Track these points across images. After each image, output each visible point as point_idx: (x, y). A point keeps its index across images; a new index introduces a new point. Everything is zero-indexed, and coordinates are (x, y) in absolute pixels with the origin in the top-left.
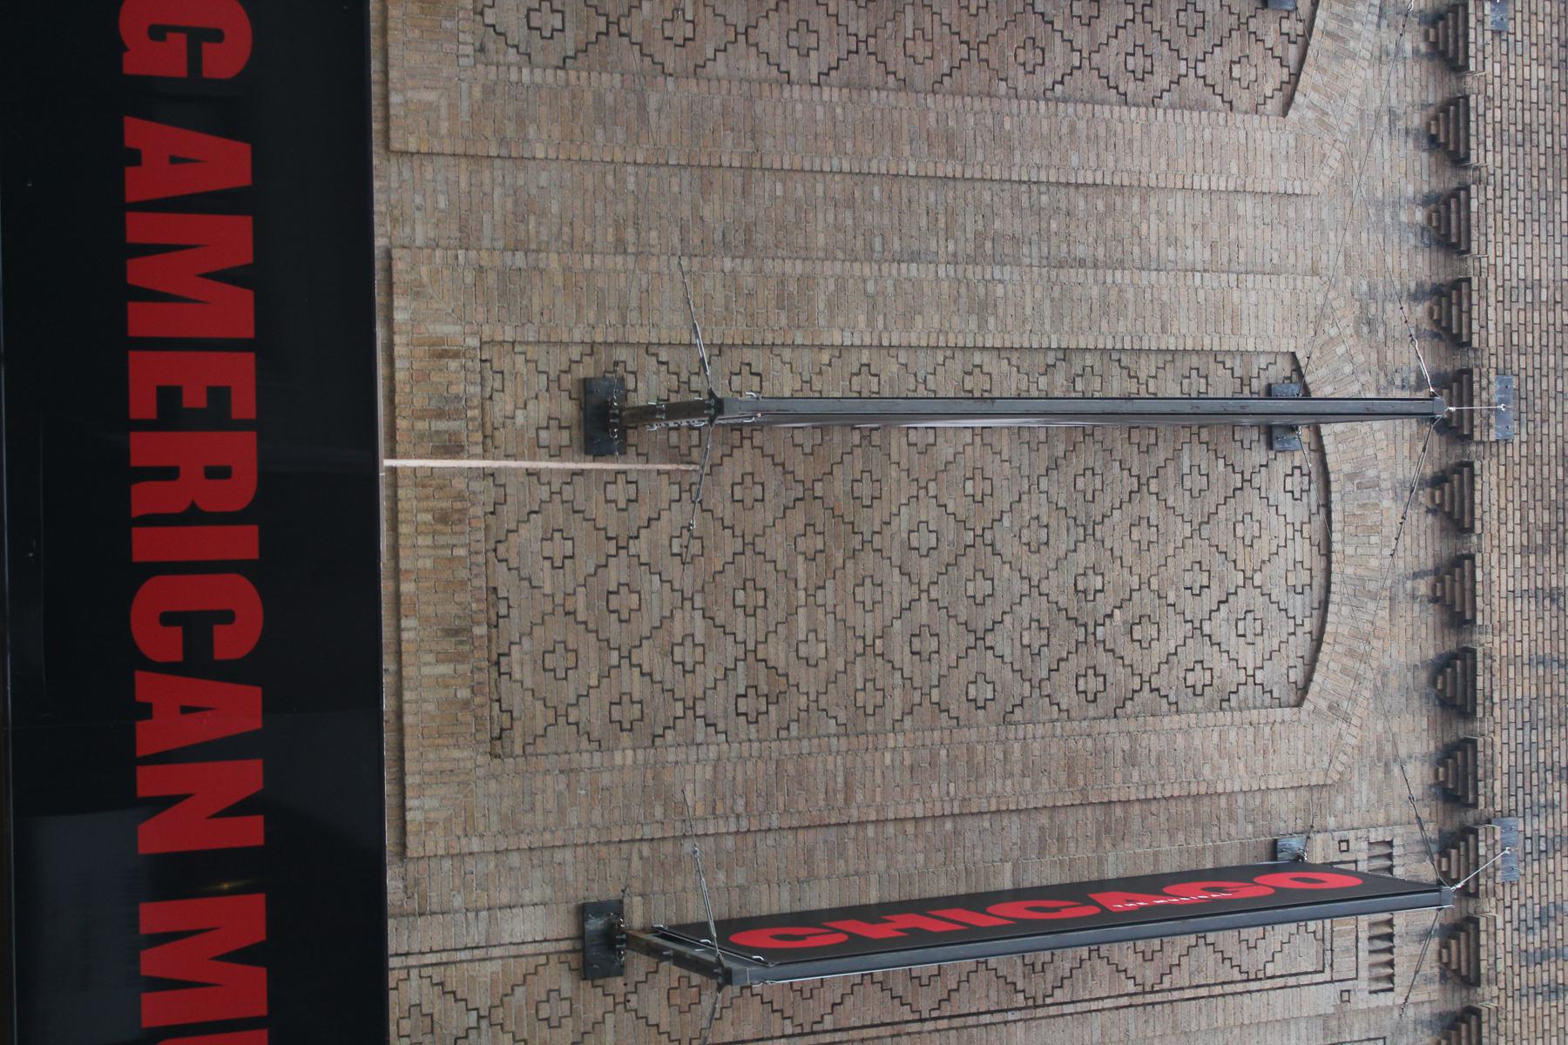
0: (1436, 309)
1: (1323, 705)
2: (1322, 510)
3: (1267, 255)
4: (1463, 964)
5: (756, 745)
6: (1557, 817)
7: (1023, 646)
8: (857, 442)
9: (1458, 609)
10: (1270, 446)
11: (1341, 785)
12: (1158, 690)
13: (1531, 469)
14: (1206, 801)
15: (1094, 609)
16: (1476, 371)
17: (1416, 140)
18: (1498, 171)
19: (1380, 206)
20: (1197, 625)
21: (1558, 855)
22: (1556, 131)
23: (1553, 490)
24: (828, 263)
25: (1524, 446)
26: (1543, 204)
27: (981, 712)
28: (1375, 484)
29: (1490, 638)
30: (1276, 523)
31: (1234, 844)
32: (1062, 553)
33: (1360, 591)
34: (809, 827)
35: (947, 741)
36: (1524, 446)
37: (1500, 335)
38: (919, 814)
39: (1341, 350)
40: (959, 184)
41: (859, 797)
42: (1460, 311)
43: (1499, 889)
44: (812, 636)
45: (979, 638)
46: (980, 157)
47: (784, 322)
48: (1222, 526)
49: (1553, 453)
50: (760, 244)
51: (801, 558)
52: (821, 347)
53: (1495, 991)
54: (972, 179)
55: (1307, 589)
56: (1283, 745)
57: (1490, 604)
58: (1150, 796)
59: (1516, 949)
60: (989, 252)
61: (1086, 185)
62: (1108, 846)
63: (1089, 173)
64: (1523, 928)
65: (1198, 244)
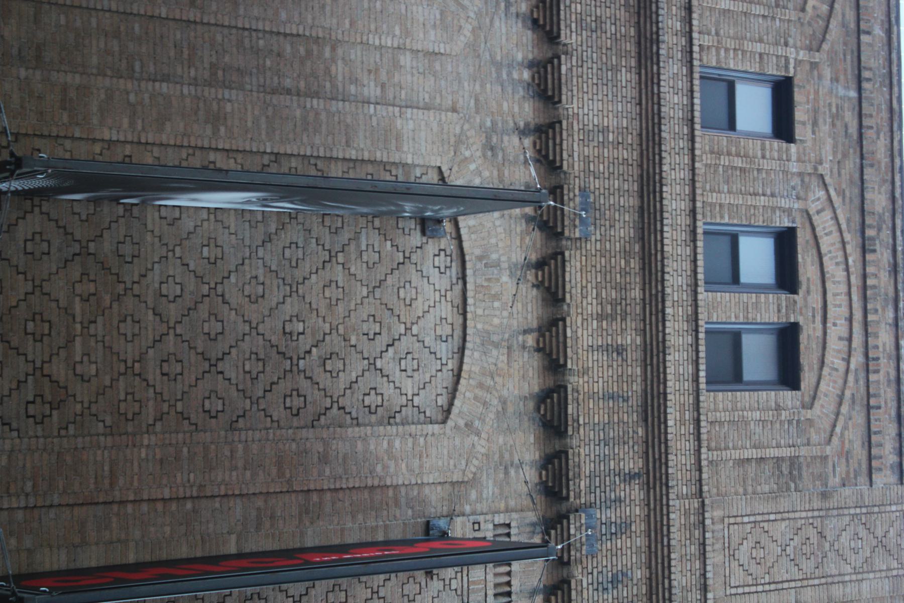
0: (538, 141)
1: (461, 423)
2: (460, 282)
3: (421, 95)
5: (41, 440)
6: (623, 508)
7: (245, 372)
8: (121, 213)
9: (554, 357)
10: (423, 233)
11: (474, 482)
12: (344, 408)
13: (603, 259)
14: (379, 490)
15: (297, 347)
16: (566, 187)
17: (524, 21)
18: (579, 48)
19: (498, 66)
20: (372, 361)
22: (618, 23)
23: (618, 276)
24: (100, 78)
25: (598, 243)
26: (610, 73)
27: (213, 420)
28: (497, 264)
29: (576, 378)
30: (428, 290)
31: (399, 524)
32: (274, 304)
33: (487, 342)
34: (82, 504)
35: (188, 441)
36: (598, 243)
37: (582, 163)
38: (167, 496)
39: (472, 167)
40: (199, 27)
41: (121, 482)
42: (555, 144)
44: (86, 359)
45: (213, 365)
46: (214, 8)
47: (65, 118)
48: (389, 290)
49: (618, 249)
50: (47, 60)
51: (77, 299)
52: (94, 140)
54: (208, 24)
55: (450, 339)
56: (433, 452)
57: (577, 354)
58: (338, 486)
60: (221, 79)
61: (292, 35)
62: (308, 524)
63: (294, 26)
64: (600, 589)
65: (372, 84)
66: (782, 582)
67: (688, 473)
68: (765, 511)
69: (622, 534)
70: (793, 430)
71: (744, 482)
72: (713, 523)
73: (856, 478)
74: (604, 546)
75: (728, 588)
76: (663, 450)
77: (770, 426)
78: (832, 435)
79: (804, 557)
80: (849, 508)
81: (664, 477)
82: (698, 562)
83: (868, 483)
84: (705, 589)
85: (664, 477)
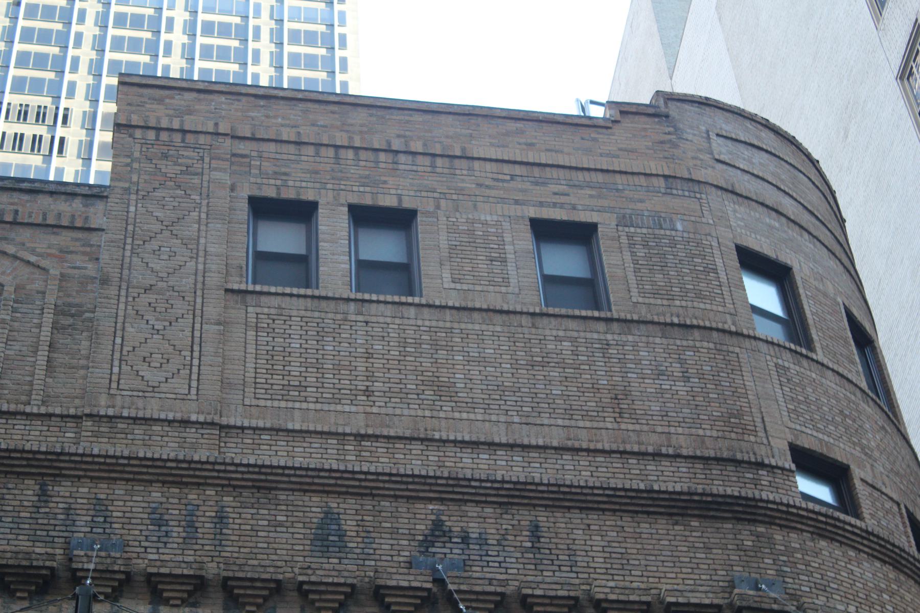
4: (184, 588)
6: (78, 506)
21: (110, 508)
43: (125, 555)
53: (214, 565)
59: (181, 546)
64: (165, 539)
66: (193, 337)
67: (51, 429)
68: (111, 347)
69: (107, 510)
70: (24, 308)
71: (73, 368)
72: (113, 407)
73: (92, 246)
74: (117, 531)
75: (189, 397)
76: (19, 455)
77: (15, 333)
78: (39, 267)
79: (169, 310)
80: (123, 256)
81: (49, 457)
82: (154, 428)
83: (100, 233)
84: (185, 423)
85: (49, 457)
